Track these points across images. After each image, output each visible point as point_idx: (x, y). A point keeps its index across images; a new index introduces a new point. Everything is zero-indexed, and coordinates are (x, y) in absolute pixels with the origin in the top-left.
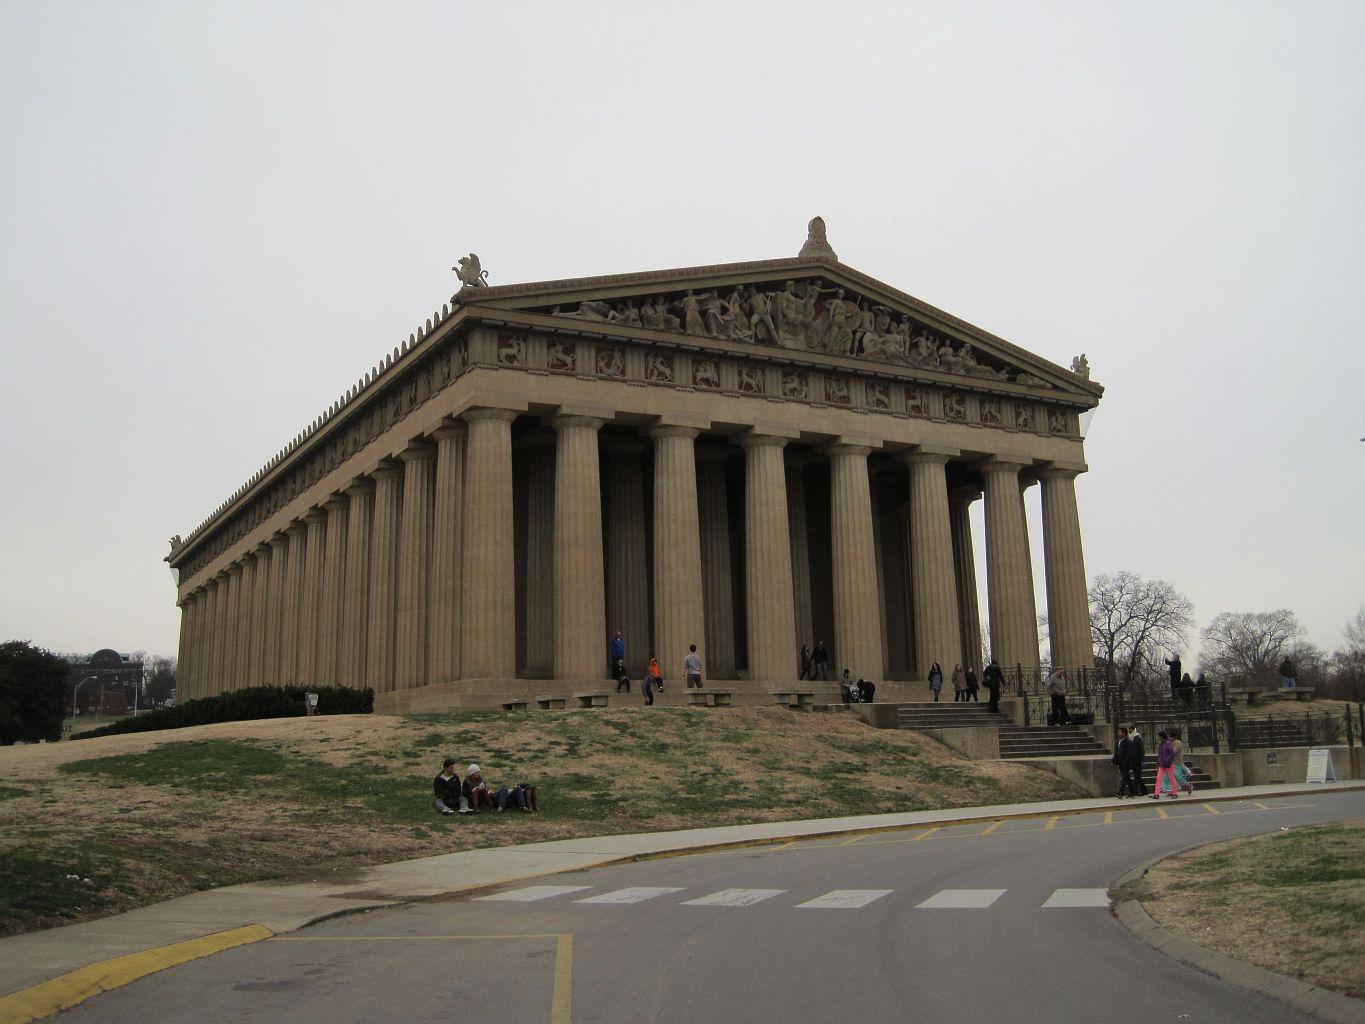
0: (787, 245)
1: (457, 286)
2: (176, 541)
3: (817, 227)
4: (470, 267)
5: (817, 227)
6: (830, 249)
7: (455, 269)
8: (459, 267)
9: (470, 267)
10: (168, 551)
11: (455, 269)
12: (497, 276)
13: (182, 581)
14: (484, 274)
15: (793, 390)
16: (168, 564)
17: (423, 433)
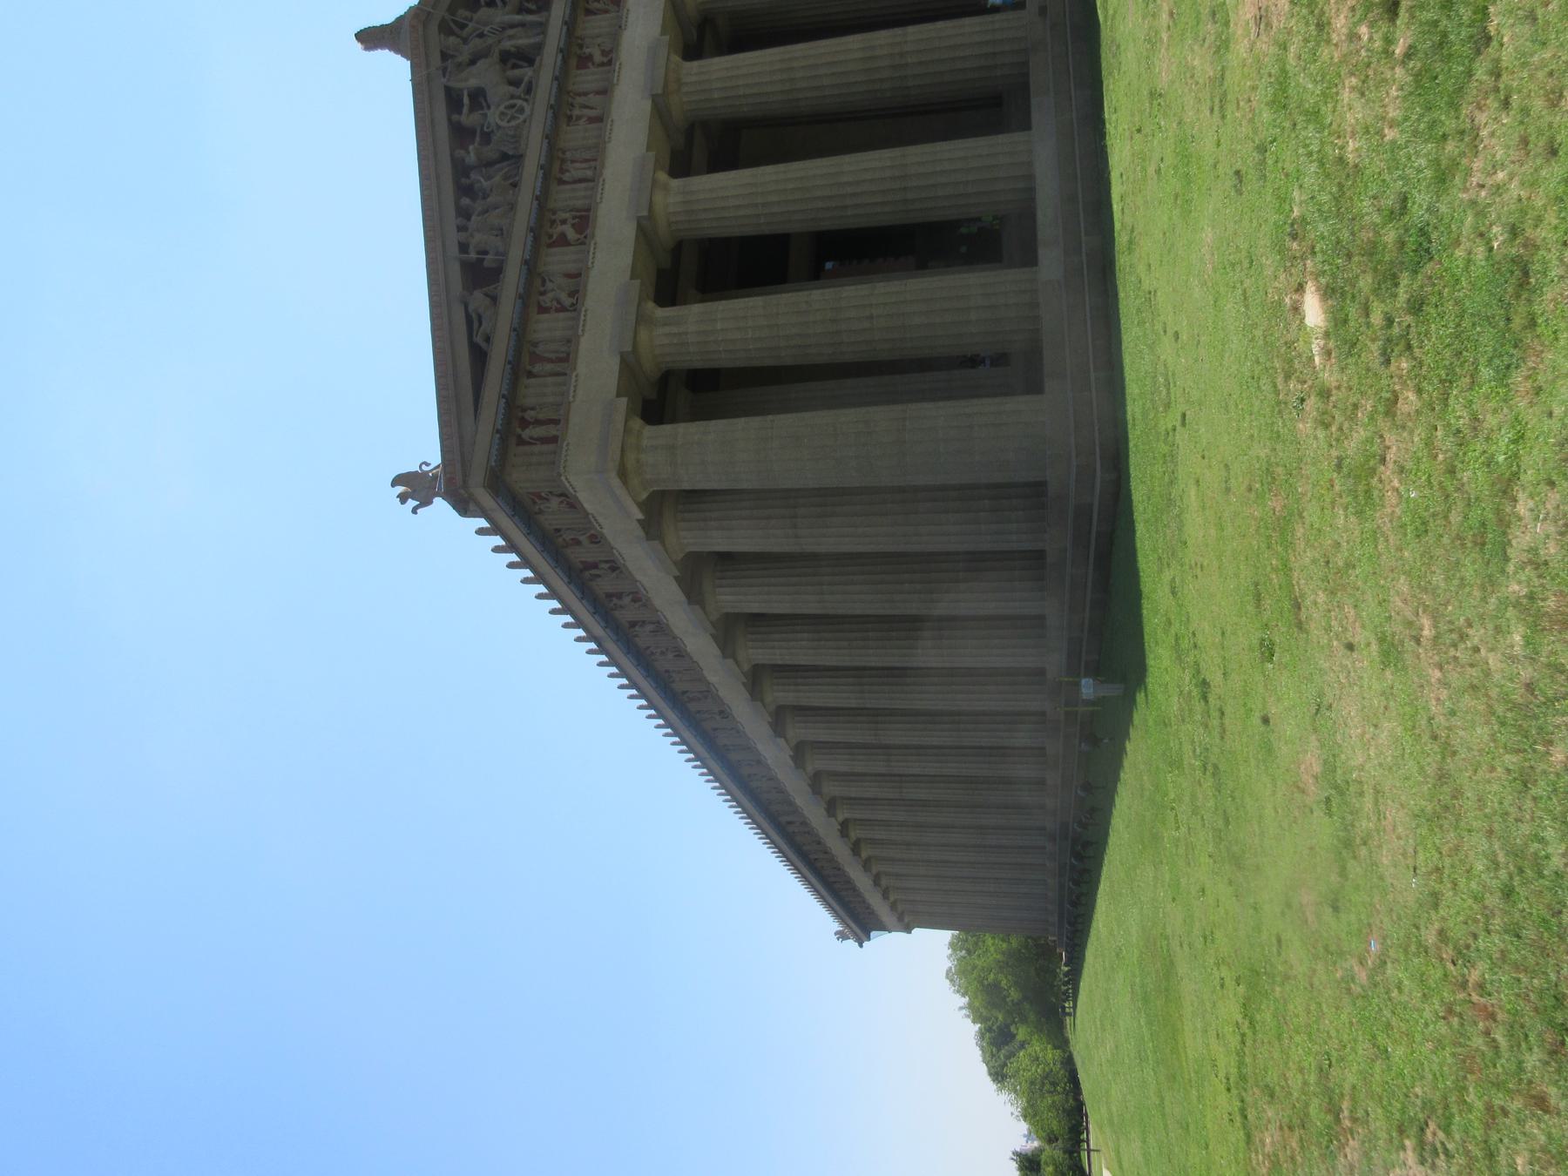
0: (395, 69)
1: (440, 506)
2: (842, 936)
3: (371, 38)
4: (415, 488)
5: (371, 38)
6: (400, 20)
7: (414, 511)
8: (412, 503)
9: (415, 488)
10: (851, 944)
11: (414, 511)
12: (427, 451)
13: (883, 928)
14: (425, 468)
15: (604, 53)
16: (866, 944)
17: (676, 578)
